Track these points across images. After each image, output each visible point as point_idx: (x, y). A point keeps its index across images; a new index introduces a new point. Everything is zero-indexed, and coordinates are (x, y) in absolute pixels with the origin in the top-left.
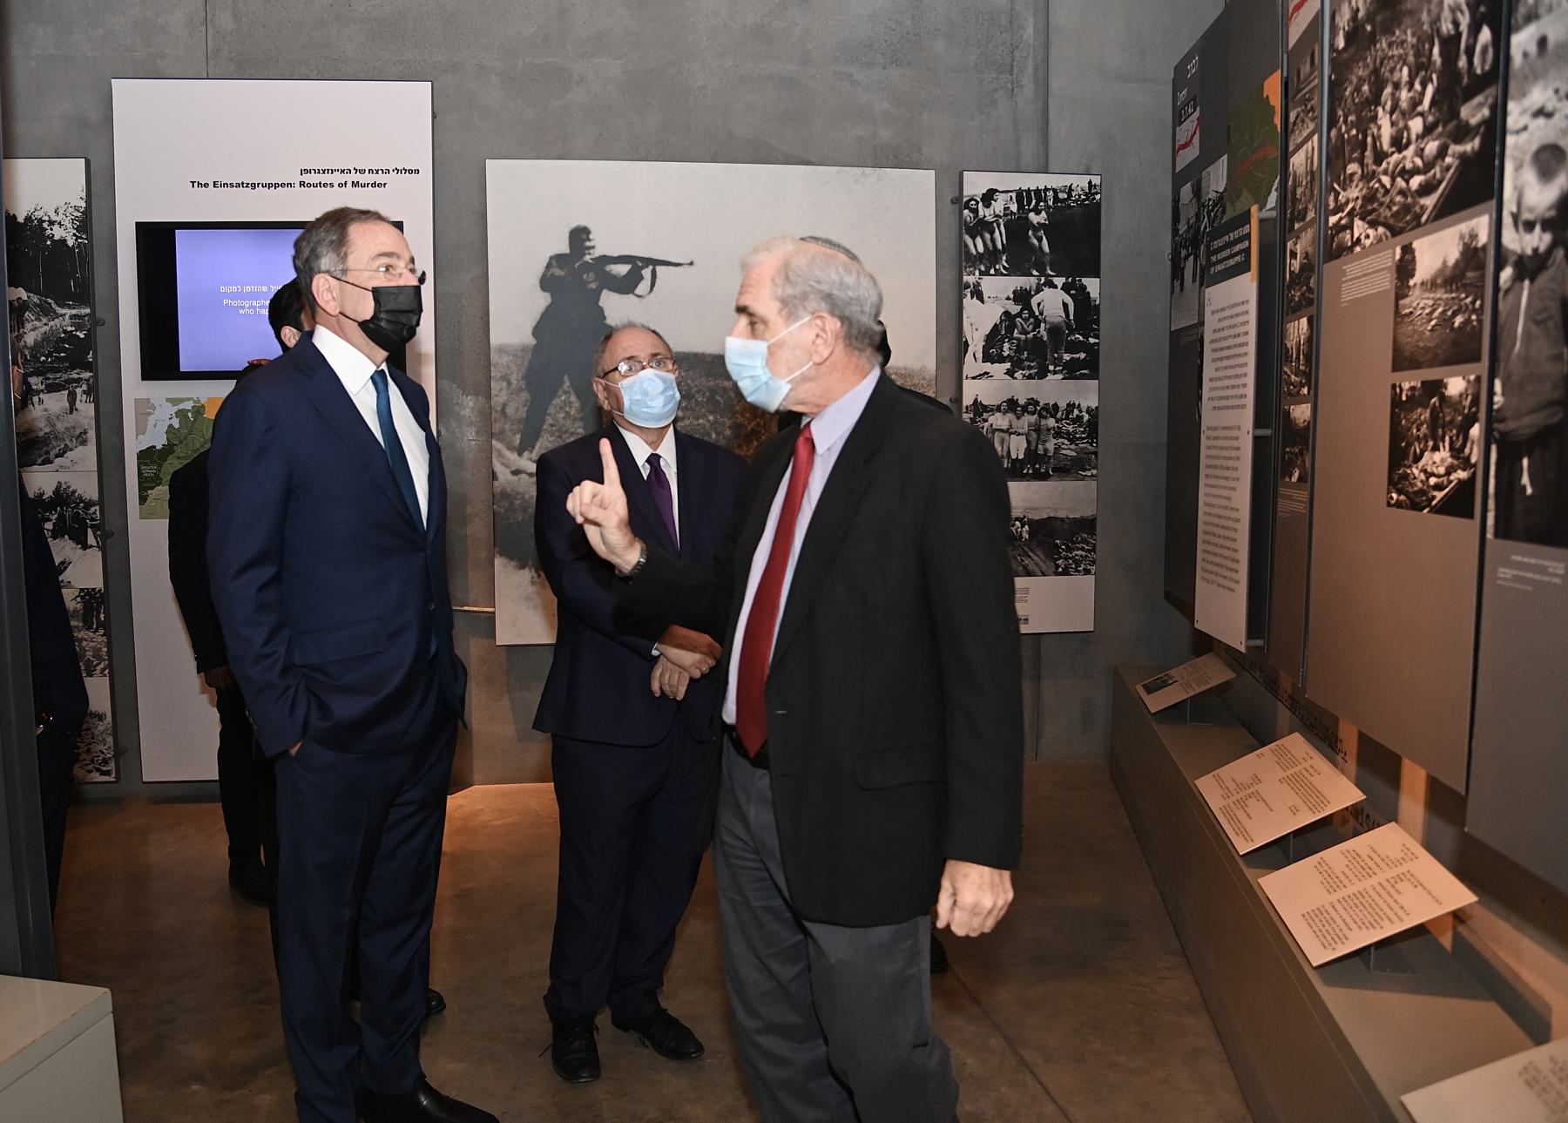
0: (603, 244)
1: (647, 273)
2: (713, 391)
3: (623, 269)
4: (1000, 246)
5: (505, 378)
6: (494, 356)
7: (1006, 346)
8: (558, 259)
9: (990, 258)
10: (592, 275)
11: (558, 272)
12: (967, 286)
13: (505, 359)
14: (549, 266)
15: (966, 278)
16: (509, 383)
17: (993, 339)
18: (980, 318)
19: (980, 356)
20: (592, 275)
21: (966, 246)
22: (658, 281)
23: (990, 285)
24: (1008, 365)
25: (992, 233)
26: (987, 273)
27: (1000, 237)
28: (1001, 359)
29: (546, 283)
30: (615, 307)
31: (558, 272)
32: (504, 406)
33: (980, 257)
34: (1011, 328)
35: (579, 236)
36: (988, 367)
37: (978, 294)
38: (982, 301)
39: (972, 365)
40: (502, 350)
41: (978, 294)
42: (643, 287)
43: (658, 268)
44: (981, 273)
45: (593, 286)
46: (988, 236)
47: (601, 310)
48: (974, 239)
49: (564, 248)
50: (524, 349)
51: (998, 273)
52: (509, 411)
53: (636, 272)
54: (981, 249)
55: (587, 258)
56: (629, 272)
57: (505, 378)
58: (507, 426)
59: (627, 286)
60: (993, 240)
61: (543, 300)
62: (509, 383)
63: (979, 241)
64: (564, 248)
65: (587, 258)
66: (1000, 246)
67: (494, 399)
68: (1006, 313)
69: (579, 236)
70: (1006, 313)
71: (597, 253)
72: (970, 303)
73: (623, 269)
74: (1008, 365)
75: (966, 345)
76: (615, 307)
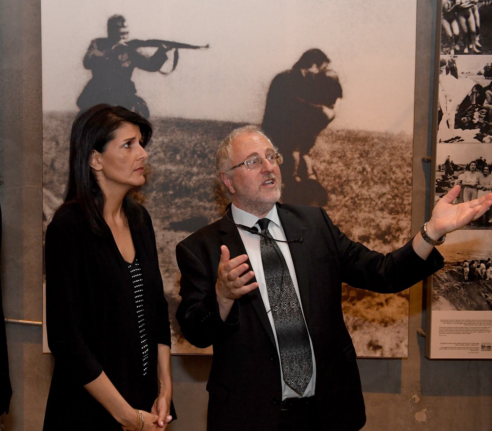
0: (135, 30)
1: (170, 54)
3: (151, 51)
4: (474, 29)
5: (55, 139)
6: (46, 122)
7: (476, 114)
8: (98, 43)
9: (466, 38)
10: (126, 56)
12: (443, 63)
13: (54, 123)
14: (91, 48)
15: (443, 57)
16: (57, 143)
17: (465, 108)
18: (453, 91)
19: (452, 123)
20: (126, 56)
21: (444, 29)
22: (180, 61)
23: (464, 62)
24: (477, 131)
25: (467, 17)
26: (461, 52)
27: (474, 21)
28: (471, 126)
29: (89, 62)
30: (144, 83)
31: (98, 53)
32: (53, 161)
33: (456, 39)
34: (480, 101)
35: (116, 24)
36: (459, 132)
37: (453, 70)
38: (456, 76)
39: (445, 131)
40: (52, 116)
41: (453, 70)
42: (167, 66)
43: (181, 51)
44: (456, 52)
45: (127, 65)
46: (463, 20)
47: (132, 85)
48: (450, 22)
49: (103, 33)
50: (69, 116)
51: (471, 52)
52: (57, 165)
53: (161, 54)
54: (457, 31)
55: (122, 42)
56: (156, 54)
57: (55, 139)
58: (55, 178)
59: (154, 65)
60: (468, 24)
61: (85, 76)
62: (57, 143)
63: (455, 24)
64: (103, 33)
65: (122, 42)
66: (474, 29)
67: (45, 156)
68: (478, 87)
69: (116, 24)
70: (478, 87)
71: (131, 37)
72: (445, 79)
73: (151, 51)
74: (477, 131)
75: (441, 114)
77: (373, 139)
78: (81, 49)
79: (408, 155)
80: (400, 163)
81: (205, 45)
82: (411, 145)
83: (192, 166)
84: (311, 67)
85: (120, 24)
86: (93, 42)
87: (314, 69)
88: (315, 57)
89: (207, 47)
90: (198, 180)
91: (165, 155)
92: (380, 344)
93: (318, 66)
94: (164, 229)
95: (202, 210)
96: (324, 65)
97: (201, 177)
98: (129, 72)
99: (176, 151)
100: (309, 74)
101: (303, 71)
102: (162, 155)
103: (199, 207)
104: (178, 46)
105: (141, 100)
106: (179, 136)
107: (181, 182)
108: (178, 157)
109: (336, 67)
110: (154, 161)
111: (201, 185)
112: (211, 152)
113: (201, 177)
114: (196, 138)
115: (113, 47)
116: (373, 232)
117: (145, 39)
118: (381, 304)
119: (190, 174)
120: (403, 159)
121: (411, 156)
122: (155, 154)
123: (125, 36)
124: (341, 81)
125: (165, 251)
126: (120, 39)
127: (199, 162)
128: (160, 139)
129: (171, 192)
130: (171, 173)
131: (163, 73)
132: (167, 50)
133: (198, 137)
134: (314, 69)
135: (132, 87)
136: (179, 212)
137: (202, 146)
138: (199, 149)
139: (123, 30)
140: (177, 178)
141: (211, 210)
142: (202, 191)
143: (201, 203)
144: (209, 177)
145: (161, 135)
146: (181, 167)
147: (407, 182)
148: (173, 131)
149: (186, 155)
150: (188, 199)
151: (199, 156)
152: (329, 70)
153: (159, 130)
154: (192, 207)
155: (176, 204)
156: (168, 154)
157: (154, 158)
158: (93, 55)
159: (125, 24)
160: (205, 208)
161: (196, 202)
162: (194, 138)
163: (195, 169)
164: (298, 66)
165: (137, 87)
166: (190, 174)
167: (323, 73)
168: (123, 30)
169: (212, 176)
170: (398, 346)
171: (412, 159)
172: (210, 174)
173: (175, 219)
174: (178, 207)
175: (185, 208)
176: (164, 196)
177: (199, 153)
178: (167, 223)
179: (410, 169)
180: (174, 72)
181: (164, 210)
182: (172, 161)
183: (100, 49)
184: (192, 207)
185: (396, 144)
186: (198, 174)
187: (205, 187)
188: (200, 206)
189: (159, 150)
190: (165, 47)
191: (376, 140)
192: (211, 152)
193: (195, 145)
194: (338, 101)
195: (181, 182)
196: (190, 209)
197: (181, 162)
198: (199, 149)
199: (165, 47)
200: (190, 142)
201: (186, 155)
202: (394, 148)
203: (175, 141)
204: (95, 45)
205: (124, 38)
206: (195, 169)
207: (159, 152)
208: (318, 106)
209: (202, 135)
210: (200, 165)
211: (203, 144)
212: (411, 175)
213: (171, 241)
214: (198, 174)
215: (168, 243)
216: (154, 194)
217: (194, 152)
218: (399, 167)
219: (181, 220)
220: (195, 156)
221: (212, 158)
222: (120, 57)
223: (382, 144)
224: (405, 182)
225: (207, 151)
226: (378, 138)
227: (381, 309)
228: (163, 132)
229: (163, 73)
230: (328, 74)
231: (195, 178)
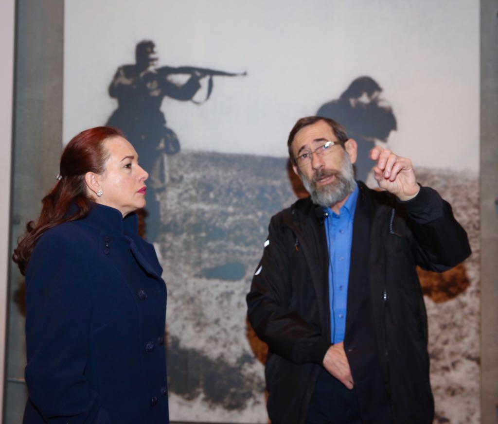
1: (204, 82)
2: (262, 190)
3: (182, 79)
8: (126, 70)
10: (155, 84)
11: (125, 81)
14: (117, 75)
20: (155, 84)
22: (215, 90)
29: (115, 90)
31: (125, 81)
35: (145, 49)
42: (200, 95)
43: (216, 79)
45: (156, 93)
49: (130, 59)
53: (193, 82)
55: (152, 69)
56: (190, 82)
59: (186, 93)
64: (130, 59)
65: (152, 69)
69: (145, 49)
76: (173, 111)
77: (433, 176)
78: (107, 76)
79: (474, 195)
80: (464, 203)
81: (242, 71)
82: (477, 184)
83: (228, 205)
84: (360, 95)
85: (149, 49)
86: (119, 69)
87: (364, 99)
88: (365, 85)
89: (245, 74)
90: (235, 222)
91: (197, 192)
92: (447, 416)
93: (370, 95)
94: (196, 276)
95: (238, 255)
96: (376, 94)
97: (237, 217)
98: (159, 100)
99: (209, 188)
100: (359, 105)
101: (352, 101)
102: (193, 193)
103: (234, 252)
104: (212, 73)
105: (171, 132)
106: (213, 172)
107: (215, 224)
108: (212, 195)
109: (388, 97)
110: (185, 200)
111: (238, 226)
112: (249, 189)
113: (237, 217)
114: (232, 173)
115: (142, 74)
116: (435, 283)
117: (176, 64)
118: (446, 369)
119: (225, 215)
120: (469, 200)
121: (477, 196)
122: (186, 191)
123: (155, 63)
124: (396, 112)
125: (196, 301)
126: (148, 66)
127: (235, 200)
128: (192, 175)
129: (203, 235)
130: (204, 212)
131: (197, 103)
132: (199, 78)
133: (235, 173)
134: (364, 99)
135: (161, 118)
136: (212, 257)
137: (239, 183)
138: (235, 186)
139: (152, 56)
140: (210, 219)
141: (248, 254)
142: (238, 233)
143: (238, 248)
144: (245, 218)
145: (193, 171)
146: (215, 207)
147: (474, 226)
148: (206, 166)
149: (220, 192)
150: (222, 242)
151: (236, 194)
152: (382, 100)
153: (192, 165)
154: (227, 252)
155: (208, 248)
156: (201, 192)
157: (185, 196)
158: (120, 85)
159: (155, 49)
160: (242, 253)
161: (231, 246)
162: (229, 174)
163: (231, 209)
164: (346, 95)
165: (168, 117)
166: (225, 215)
167: (374, 103)
168: (152, 56)
169: (250, 217)
170: (468, 419)
171: (479, 200)
172: (246, 214)
173: (207, 265)
174: (211, 252)
175: (219, 253)
176: (196, 239)
177: (235, 191)
178: (198, 270)
179: (476, 211)
180: (209, 102)
181: (196, 255)
182: (205, 199)
183: (127, 76)
184: (227, 252)
185: (459, 182)
186: (233, 214)
187: (241, 230)
188: (237, 251)
189: (191, 186)
190: (198, 74)
191: (436, 178)
192: (249, 189)
193: (231, 182)
194: (393, 135)
195: (215, 224)
196: (224, 254)
197: (215, 201)
198: (235, 186)
199: (198, 74)
200: (225, 178)
201: (220, 192)
202: (458, 187)
203: (208, 177)
204: (122, 72)
205: (153, 65)
206: (231, 209)
207: (190, 189)
208: (370, 139)
209: (239, 171)
210: (236, 205)
211: (240, 181)
212: (477, 218)
213: (203, 290)
214: (233, 214)
215: (199, 292)
216: (184, 236)
217: (229, 190)
218: (464, 208)
219: (213, 266)
220: (231, 194)
221: (250, 196)
222: (149, 85)
223: (443, 183)
224: (471, 225)
225: (244, 188)
226: (439, 176)
227: (447, 375)
228: (195, 166)
229: (197, 103)
230: (381, 104)
231: (230, 219)
